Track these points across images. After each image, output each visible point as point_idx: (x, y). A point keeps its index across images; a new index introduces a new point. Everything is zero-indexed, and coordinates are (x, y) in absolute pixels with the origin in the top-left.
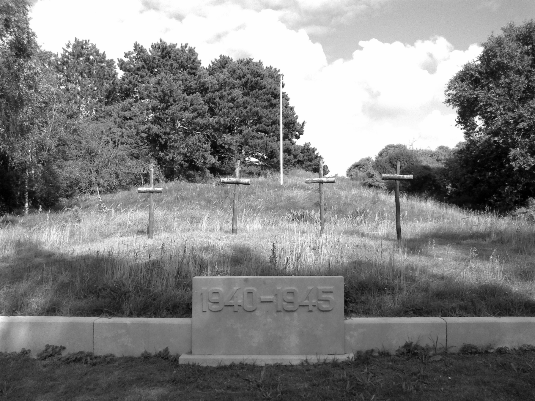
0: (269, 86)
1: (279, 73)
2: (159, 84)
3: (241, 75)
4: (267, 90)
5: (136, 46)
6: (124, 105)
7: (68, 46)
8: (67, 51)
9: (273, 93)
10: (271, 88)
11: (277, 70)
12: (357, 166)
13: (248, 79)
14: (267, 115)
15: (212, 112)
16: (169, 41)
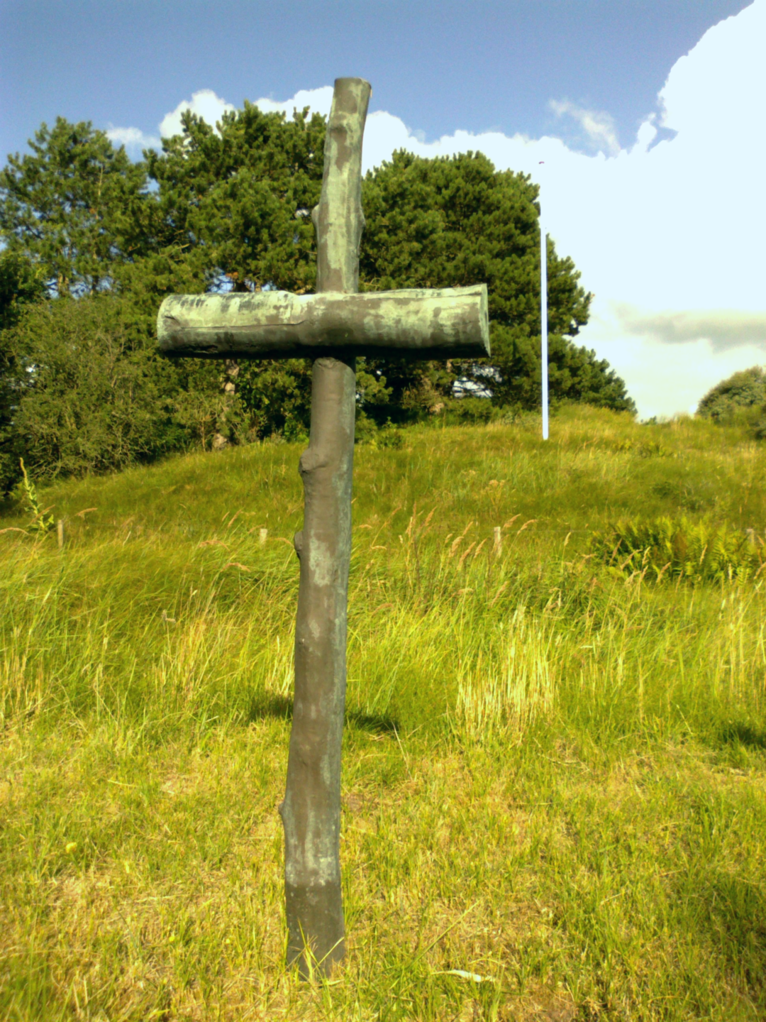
0: (508, 204)
1: (529, 182)
3: (442, 182)
4: (504, 212)
6: (160, 261)
7: (41, 138)
9: (518, 221)
10: (512, 208)
11: (526, 175)
12: (726, 390)
13: (458, 189)
14: (505, 273)
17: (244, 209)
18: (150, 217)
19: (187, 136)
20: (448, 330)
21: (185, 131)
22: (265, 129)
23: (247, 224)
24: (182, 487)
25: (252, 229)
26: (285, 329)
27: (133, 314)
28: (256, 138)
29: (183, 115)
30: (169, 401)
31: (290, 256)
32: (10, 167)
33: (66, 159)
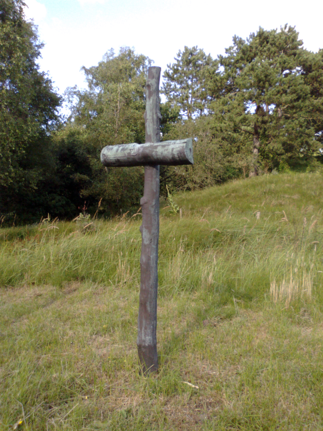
5: (235, 39)
7: (179, 55)
8: (178, 60)
16: (267, 28)
17: (257, 75)
18: (221, 82)
19: (235, 46)
20: (176, 156)
21: (234, 44)
22: (267, 38)
23: (260, 81)
24: (230, 195)
25: (262, 82)
26: (132, 157)
27: (215, 123)
28: (263, 43)
29: (233, 37)
30: (230, 158)
31: (278, 92)
32: (168, 69)
33: (188, 62)
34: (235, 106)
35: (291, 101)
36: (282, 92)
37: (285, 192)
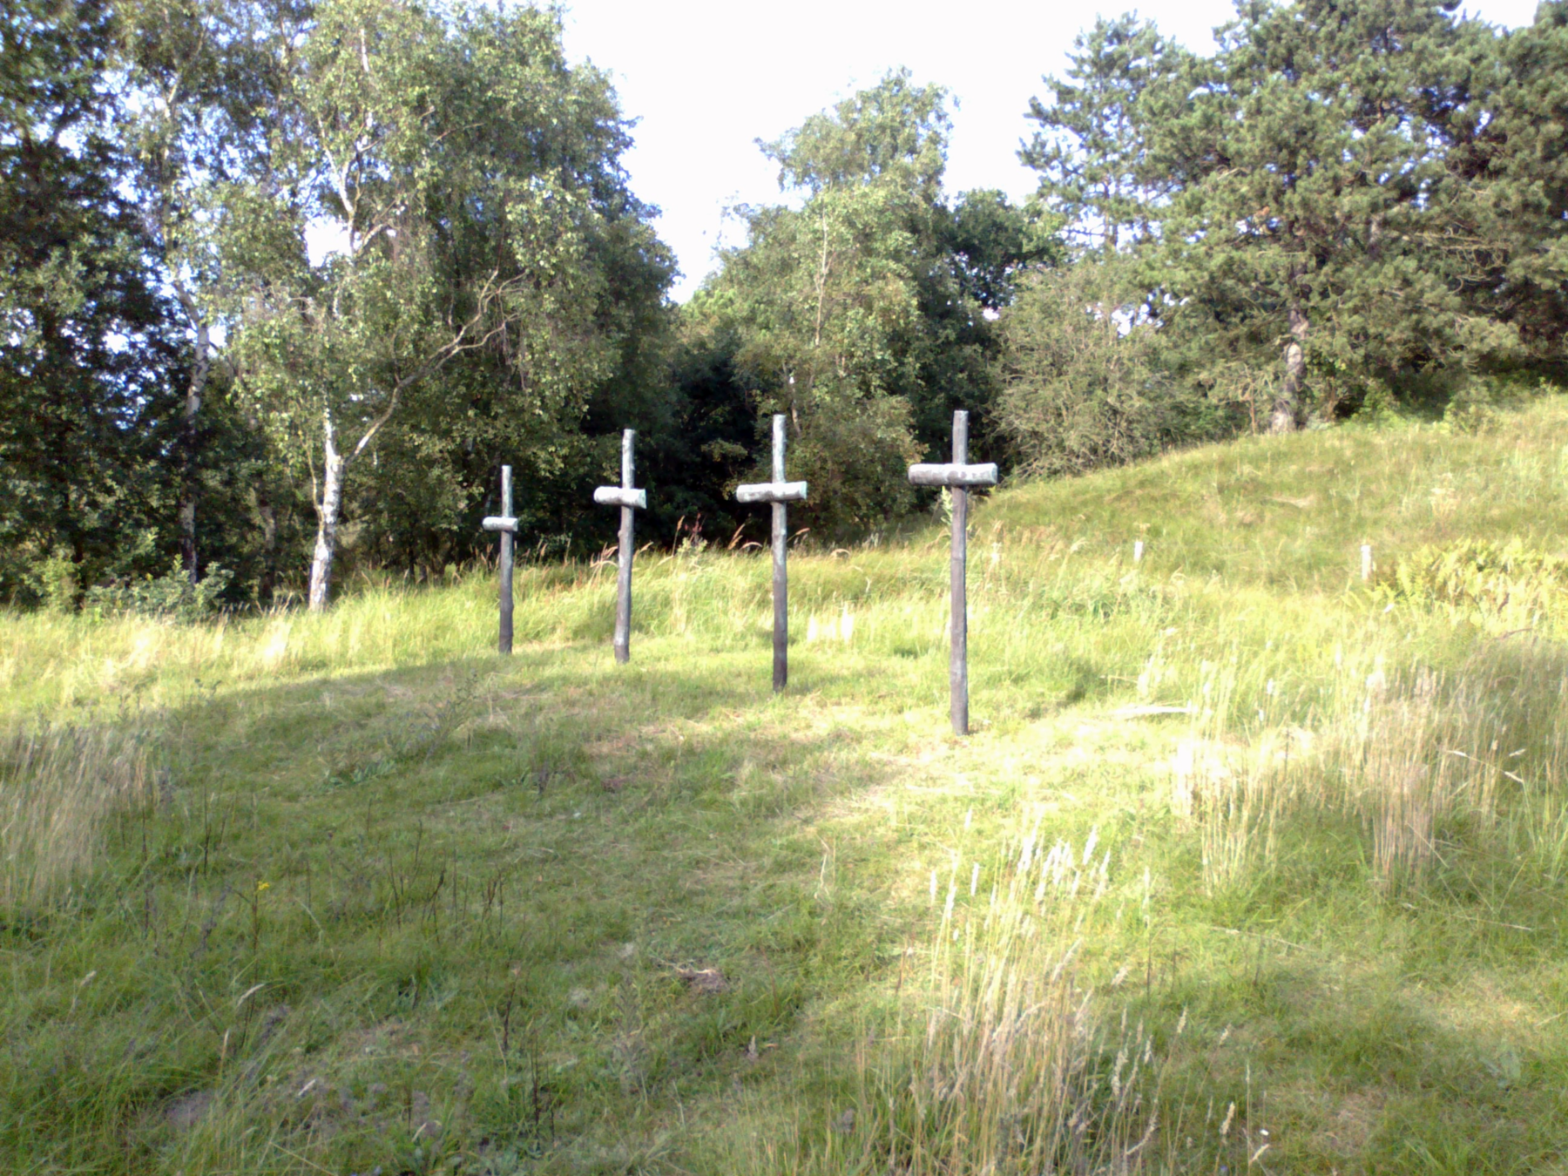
2: (1259, 112)
7: (1080, 43)
15: (1476, 167)
17: (1269, 129)
30: (1204, 376)
33: (1105, 66)
34: (1217, 217)
35: (1374, 207)
36: (1350, 177)
37: (1284, 487)
